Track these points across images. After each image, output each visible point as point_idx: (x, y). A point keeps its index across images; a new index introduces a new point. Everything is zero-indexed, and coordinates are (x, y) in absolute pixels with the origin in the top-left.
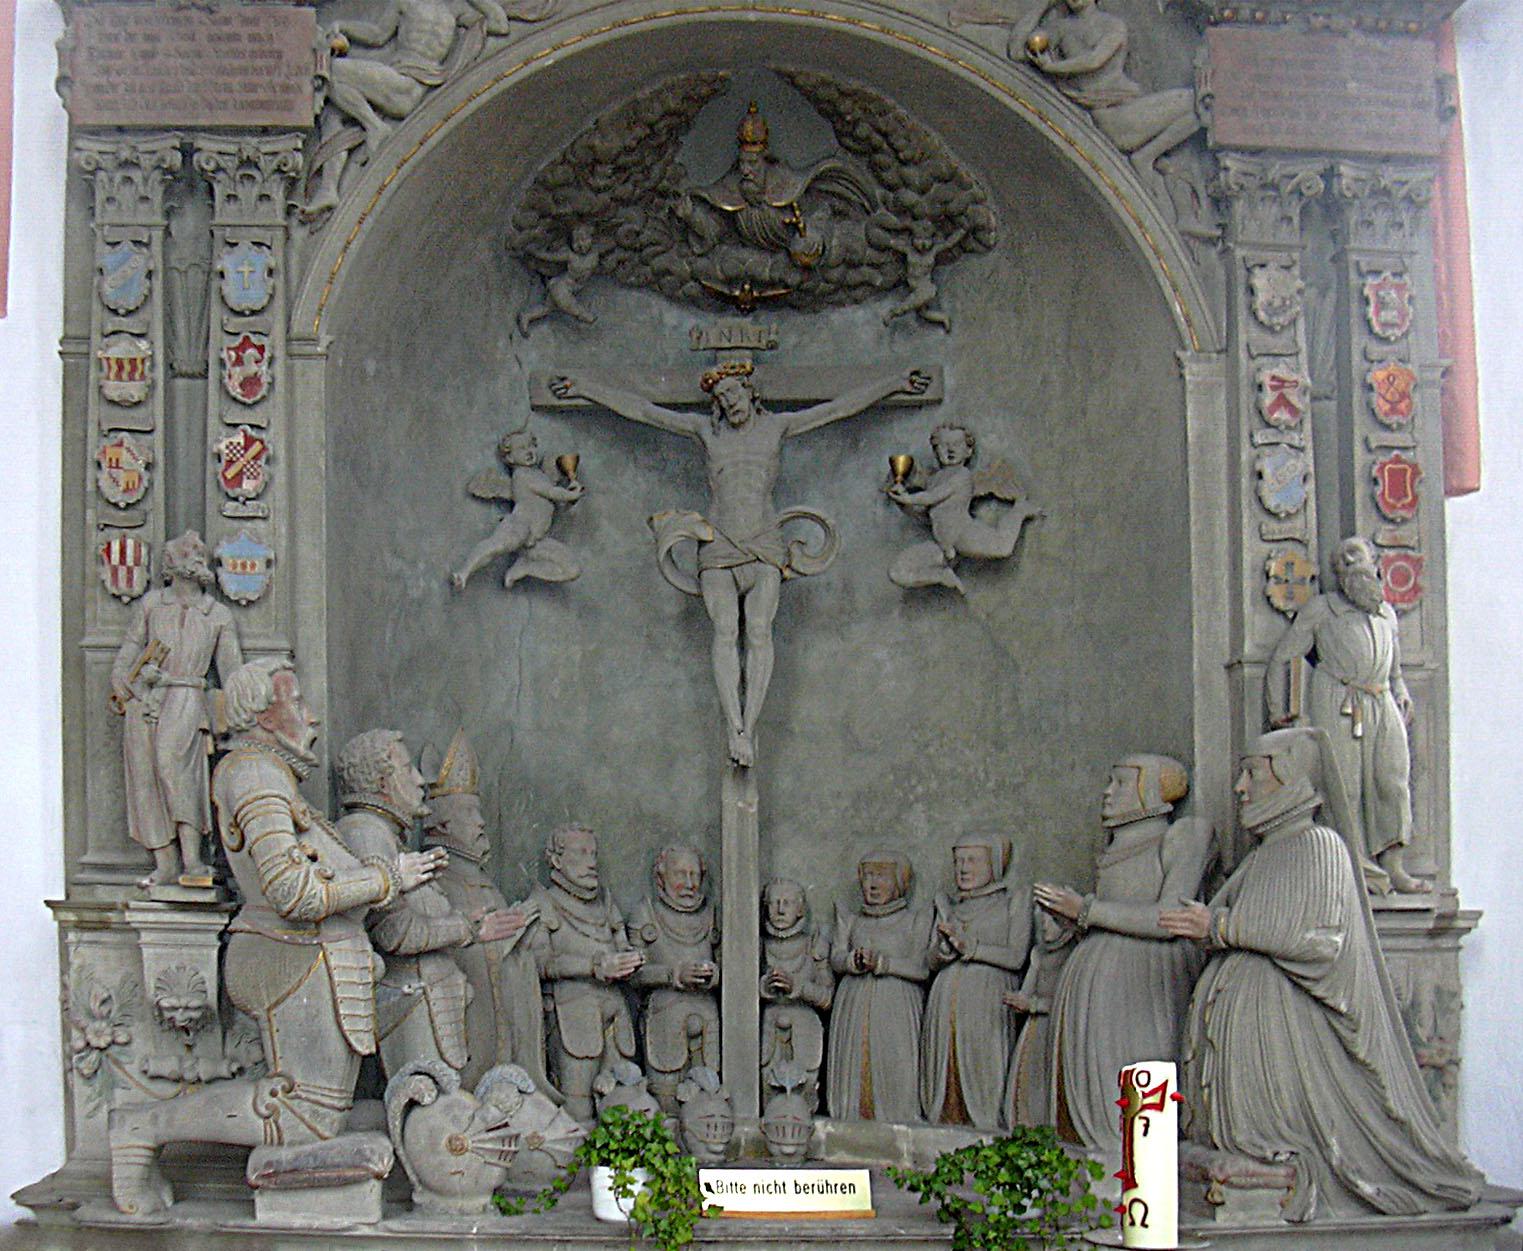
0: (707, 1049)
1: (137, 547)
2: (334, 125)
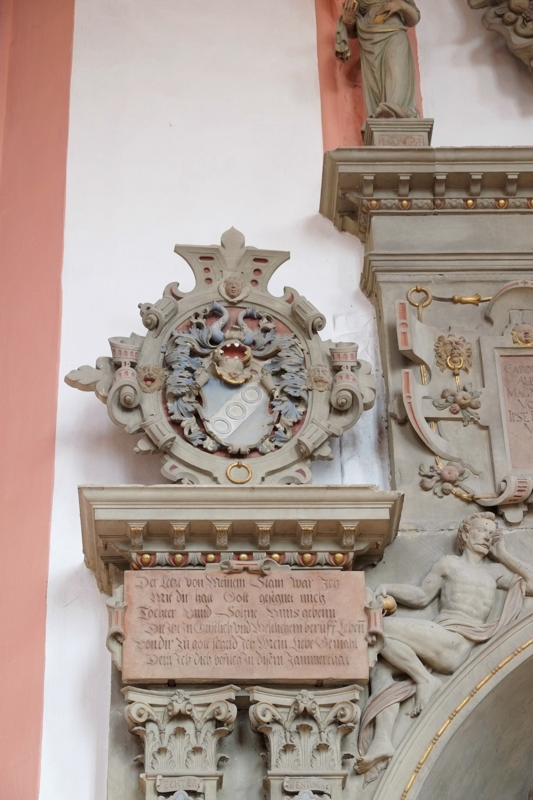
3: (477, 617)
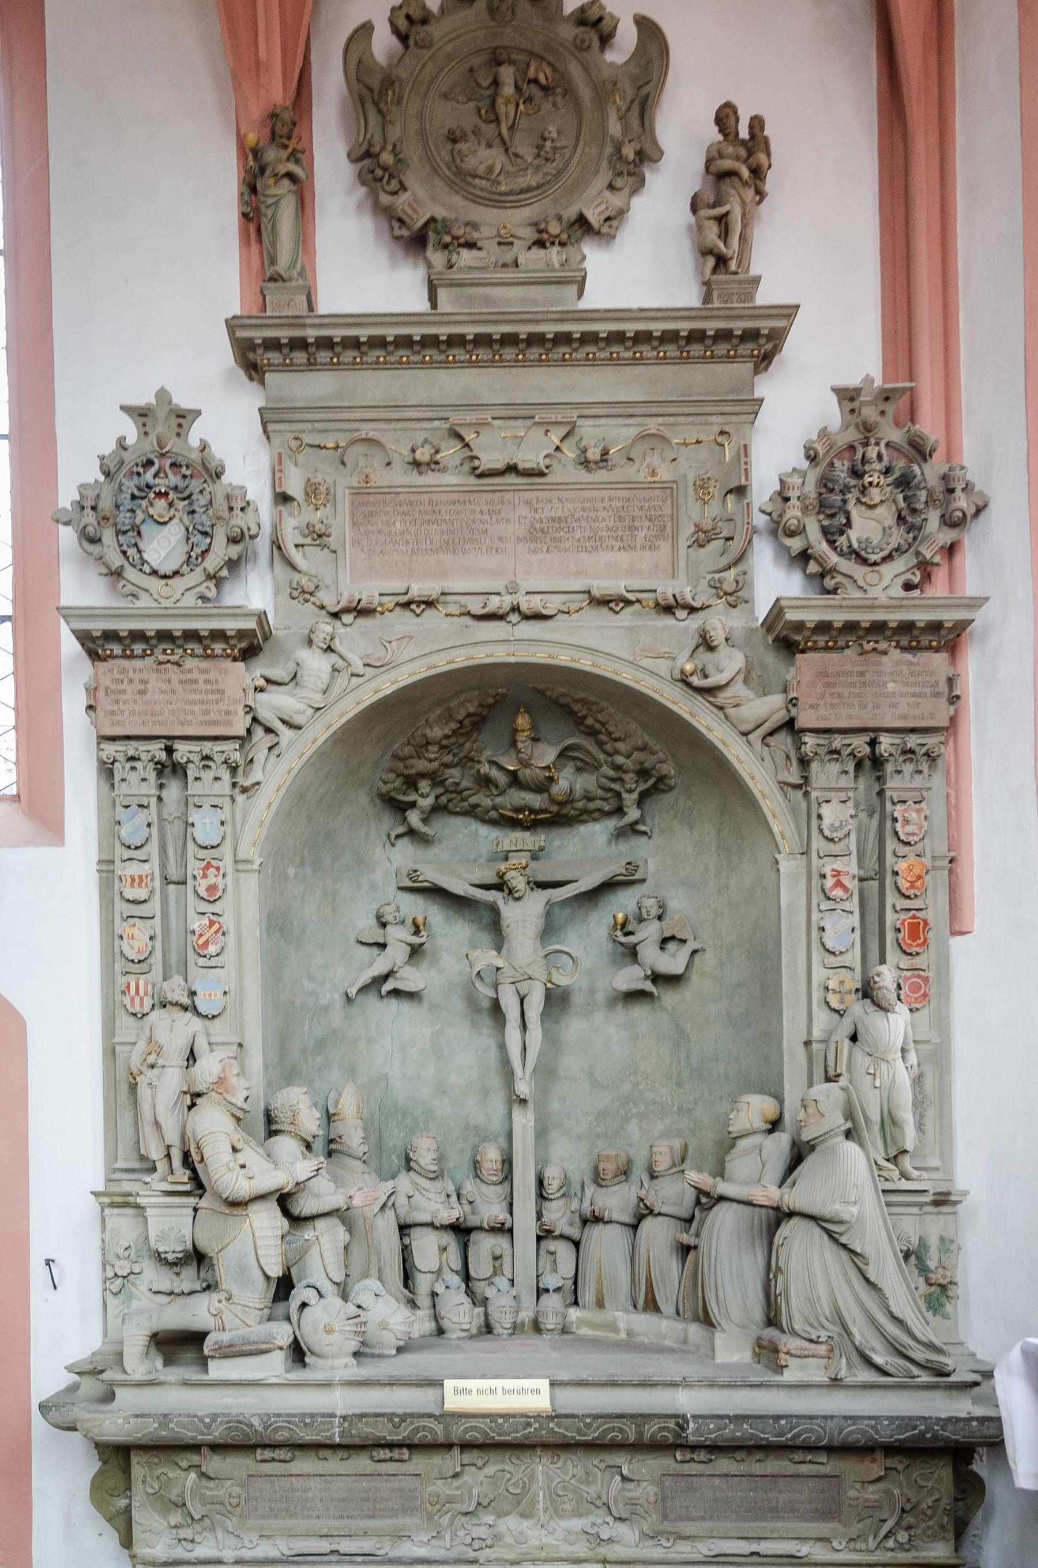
0: (504, 1266)
1: (146, 984)
2: (259, 732)
3: (317, 692)
